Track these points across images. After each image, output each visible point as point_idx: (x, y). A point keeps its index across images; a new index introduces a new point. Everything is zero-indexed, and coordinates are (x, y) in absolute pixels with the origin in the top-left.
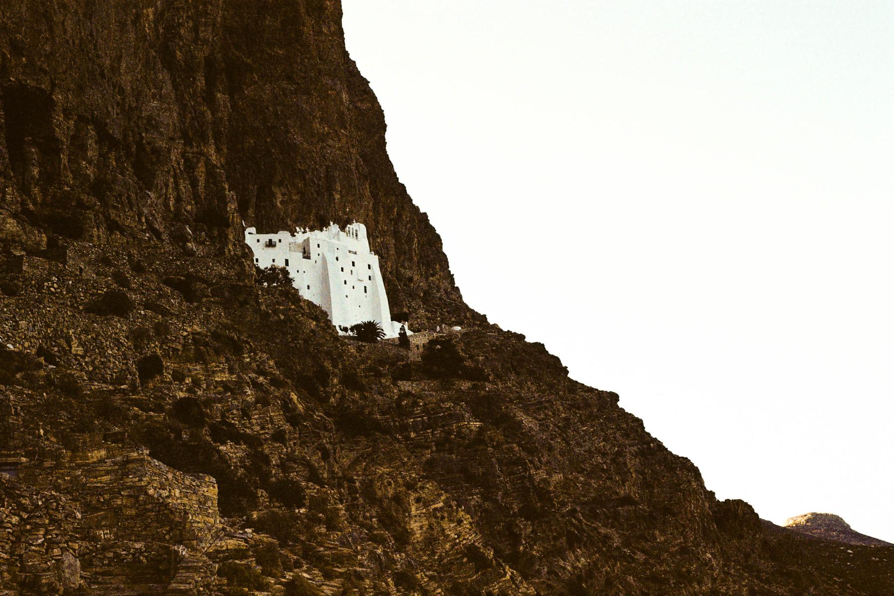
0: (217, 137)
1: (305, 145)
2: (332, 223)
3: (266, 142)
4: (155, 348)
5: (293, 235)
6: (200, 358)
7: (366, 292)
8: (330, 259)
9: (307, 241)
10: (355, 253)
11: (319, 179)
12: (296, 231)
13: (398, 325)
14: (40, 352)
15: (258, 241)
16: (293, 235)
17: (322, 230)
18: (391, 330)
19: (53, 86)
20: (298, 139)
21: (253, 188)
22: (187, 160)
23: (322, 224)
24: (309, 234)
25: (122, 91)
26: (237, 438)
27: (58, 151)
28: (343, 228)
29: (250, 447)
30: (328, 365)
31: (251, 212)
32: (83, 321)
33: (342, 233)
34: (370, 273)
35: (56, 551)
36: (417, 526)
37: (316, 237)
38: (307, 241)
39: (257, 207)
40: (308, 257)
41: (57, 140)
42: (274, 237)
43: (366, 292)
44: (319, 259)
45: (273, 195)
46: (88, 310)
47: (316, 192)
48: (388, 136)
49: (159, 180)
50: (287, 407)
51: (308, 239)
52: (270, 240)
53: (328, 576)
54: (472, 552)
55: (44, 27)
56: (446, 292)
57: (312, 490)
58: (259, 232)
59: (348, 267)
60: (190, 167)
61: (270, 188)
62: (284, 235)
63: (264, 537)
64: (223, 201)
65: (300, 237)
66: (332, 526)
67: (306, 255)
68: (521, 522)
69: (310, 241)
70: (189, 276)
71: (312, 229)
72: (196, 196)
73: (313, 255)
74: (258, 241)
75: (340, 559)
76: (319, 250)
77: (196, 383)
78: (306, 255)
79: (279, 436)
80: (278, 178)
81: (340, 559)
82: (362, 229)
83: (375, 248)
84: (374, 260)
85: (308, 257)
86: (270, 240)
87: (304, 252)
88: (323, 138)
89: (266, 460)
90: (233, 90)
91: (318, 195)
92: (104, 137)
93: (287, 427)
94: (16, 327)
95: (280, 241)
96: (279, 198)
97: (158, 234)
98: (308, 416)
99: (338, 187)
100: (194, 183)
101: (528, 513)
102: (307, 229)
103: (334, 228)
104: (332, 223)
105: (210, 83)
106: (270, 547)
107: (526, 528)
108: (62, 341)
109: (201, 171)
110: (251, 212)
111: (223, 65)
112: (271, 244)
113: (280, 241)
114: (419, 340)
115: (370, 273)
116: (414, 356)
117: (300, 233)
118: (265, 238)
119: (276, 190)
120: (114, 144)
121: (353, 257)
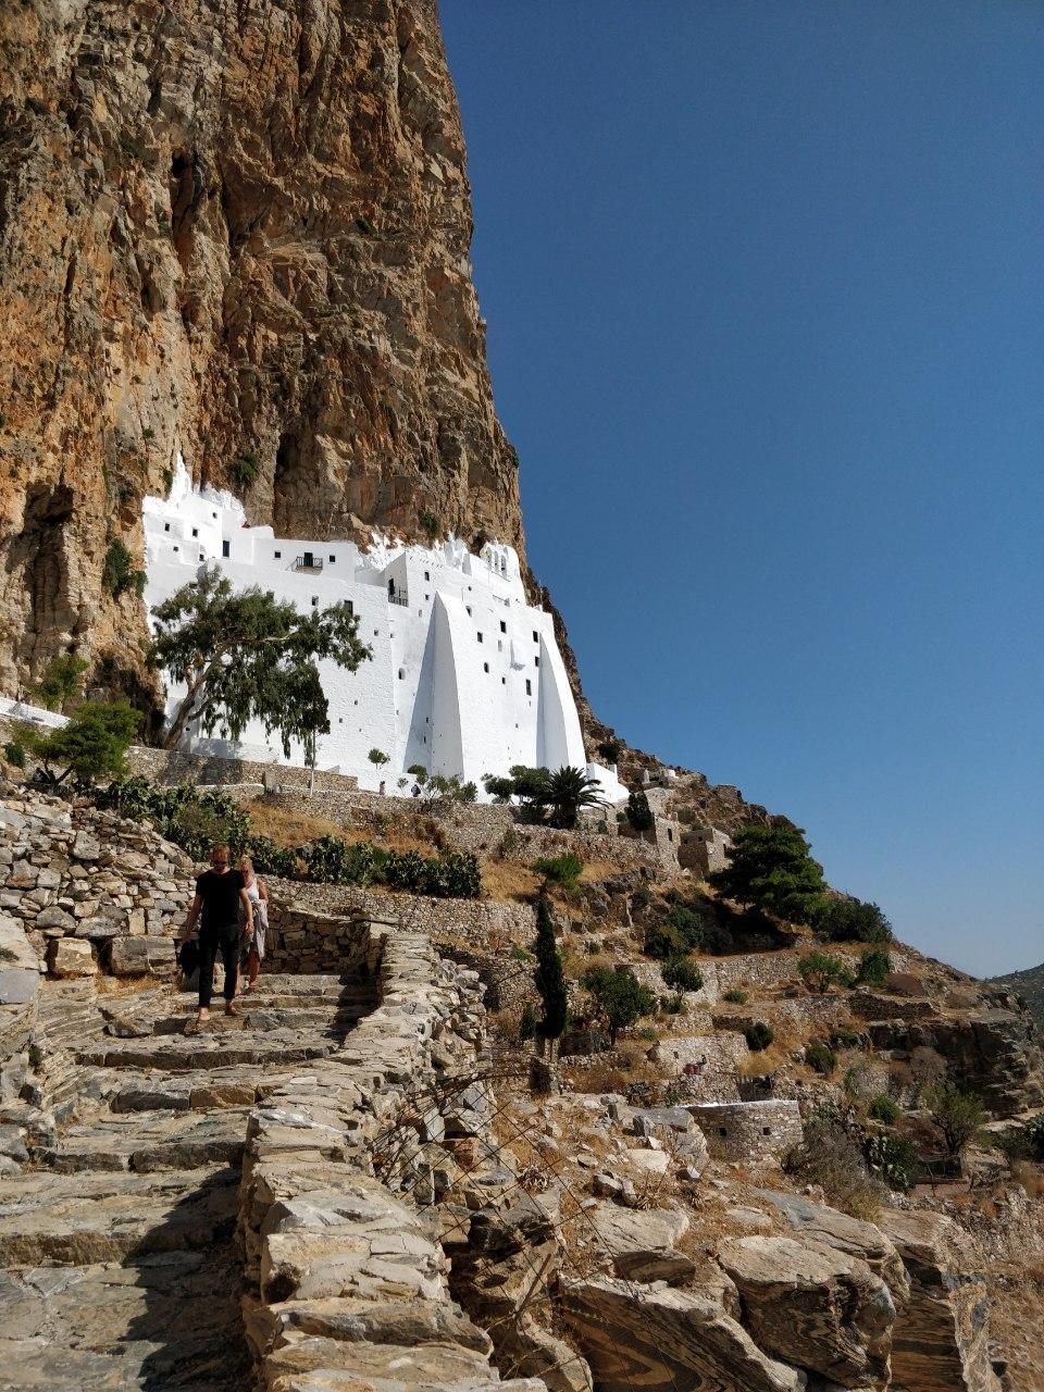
0: (188, 314)
1: (395, 361)
2: (451, 535)
3: (307, 340)
5: (364, 550)
8: (454, 608)
10: (507, 603)
12: (371, 541)
15: (278, 555)
16: (364, 550)
20: (383, 345)
21: (270, 434)
31: (263, 488)
33: (473, 557)
37: (419, 557)
39: (279, 482)
40: (403, 602)
42: (320, 550)
44: (428, 608)
45: (317, 452)
47: (419, 462)
52: (308, 558)
59: (493, 634)
61: (313, 438)
62: (345, 549)
67: (396, 593)
69: (408, 563)
73: (415, 596)
74: (278, 555)
78: (396, 593)
80: (329, 418)
84: (544, 622)
85: (403, 602)
86: (308, 558)
87: (392, 590)
88: (430, 361)
90: (239, 238)
91: (421, 469)
95: (332, 559)
96: (333, 460)
99: (464, 461)
102: (398, 541)
104: (451, 535)
111: (216, 178)
113: (332, 559)
115: (535, 649)
117: (382, 548)
118: (295, 548)
119: (325, 442)
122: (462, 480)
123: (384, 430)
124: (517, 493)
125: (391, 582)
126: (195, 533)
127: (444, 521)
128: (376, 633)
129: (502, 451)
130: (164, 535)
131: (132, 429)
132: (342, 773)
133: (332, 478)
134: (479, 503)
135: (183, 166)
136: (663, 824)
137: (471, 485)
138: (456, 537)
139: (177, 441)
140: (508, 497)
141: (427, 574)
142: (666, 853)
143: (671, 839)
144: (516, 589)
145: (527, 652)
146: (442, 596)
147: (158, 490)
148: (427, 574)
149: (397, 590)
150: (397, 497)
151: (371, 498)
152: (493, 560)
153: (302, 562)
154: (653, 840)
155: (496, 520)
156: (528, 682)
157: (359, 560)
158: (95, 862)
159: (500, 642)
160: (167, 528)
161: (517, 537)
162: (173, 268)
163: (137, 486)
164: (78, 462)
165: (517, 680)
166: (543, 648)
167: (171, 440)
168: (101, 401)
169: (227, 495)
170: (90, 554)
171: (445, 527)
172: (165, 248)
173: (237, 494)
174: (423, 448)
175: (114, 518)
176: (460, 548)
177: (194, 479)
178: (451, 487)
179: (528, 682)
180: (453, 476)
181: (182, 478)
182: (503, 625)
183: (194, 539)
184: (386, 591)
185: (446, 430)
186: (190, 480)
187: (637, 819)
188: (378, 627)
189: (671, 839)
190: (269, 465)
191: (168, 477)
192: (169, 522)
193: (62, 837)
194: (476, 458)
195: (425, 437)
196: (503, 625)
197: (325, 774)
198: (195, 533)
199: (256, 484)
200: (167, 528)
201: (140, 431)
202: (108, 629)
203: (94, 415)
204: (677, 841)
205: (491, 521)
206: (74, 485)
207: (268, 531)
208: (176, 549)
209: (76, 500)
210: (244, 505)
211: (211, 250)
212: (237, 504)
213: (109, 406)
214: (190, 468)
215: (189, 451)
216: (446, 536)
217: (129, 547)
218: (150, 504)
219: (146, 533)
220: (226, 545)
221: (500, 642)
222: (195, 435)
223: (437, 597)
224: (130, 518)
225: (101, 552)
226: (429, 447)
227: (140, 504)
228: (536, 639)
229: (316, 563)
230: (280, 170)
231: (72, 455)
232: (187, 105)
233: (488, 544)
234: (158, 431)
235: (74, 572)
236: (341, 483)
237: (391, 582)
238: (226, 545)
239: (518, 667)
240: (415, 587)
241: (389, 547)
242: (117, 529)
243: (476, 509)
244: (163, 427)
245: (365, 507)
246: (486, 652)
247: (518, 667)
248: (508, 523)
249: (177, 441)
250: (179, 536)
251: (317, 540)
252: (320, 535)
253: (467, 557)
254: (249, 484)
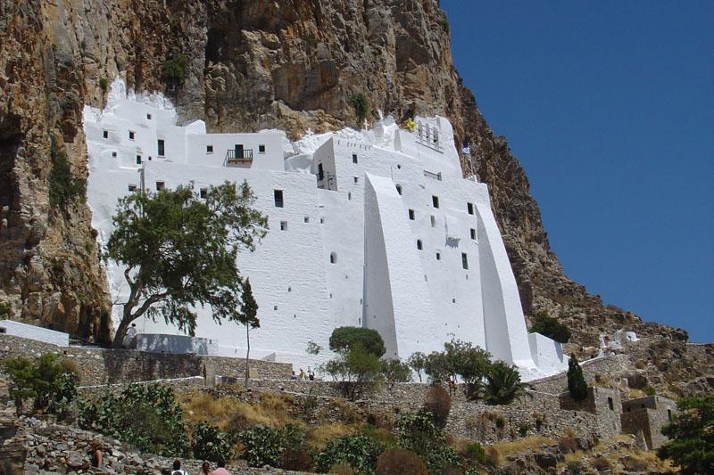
7: (465, 266)
8: (384, 186)
9: (328, 148)
10: (439, 176)
11: (349, 16)
15: (210, 149)
16: (294, 138)
17: (358, 127)
23: (361, 113)
24: (327, 135)
28: (402, 123)
33: (403, 133)
34: (472, 222)
37: (347, 139)
38: (328, 148)
42: (250, 141)
43: (465, 266)
45: (245, 45)
47: (345, 43)
51: (331, 140)
52: (239, 149)
56: (543, 263)
58: (215, 126)
62: (273, 137)
65: (311, 143)
67: (324, 177)
69: (335, 146)
71: (337, 124)
74: (210, 149)
76: (355, 170)
78: (324, 177)
84: (479, 193)
86: (239, 149)
87: (321, 176)
91: (347, 49)
95: (262, 149)
96: (260, 50)
112: (239, 156)
113: (262, 149)
117: (309, 131)
118: (226, 141)
119: (251, 36)
121: (434, 188)
122: (389, 58)
123: (308, 18)
124: (450, 60)
125: (320, 166)
126: (132, 136)
127: (374, 99)
128: (306, 220)
129: (431, 18)
130: (102, 143)
131: (67, 46)
132: (277, 360)
133: (259, 68)
134: (409, 75)
136: (601, 394)
137: (399, 61)
138: (385, 115)
139: (110, 48)
140: (439, 62)
141: (355, 157)
142: (607, 425)
143: (612, 408)
144: (448, 160)
146: (369, 176)
147: (95, 99)
148: (355, 157)
149: (325, 174)
150: (323, 81)
151: (298, 84)
152: (424, 133)
153: (233, 155)
154: (591, 408)
155: (427, 91)
156: (464, 256)
157: (288, 147)
158: (79, 467)
159: (432, 218)
160: (106, 135)
161: (450, 105)
163: (76, 98)
164: (24, 90)
165: (453, 255)
166: (480, 223)
167: (104, 48)
168: (39, 27)
169: (160, 97)
170: (37, 172)
171: (374, 106)
173: (167, 94)
174: (348, 28)
175: (57, 132)
176: (389, 127)
177: (129, 83)
178: (378, 67)
179: (464, 256)
180: (380, 53)
181: (118, 85)
182: (435, 200)
183: (131, 141)
184: (314, 177)
185: (372, 6)
186: (124, 84)
187: (577, 392)
188: (309, 214)
189: (612, 408)
191: (104, 86)
192: (106, 129)
193: (62, 454)
194: (403, 31)
195: (349, 16)
196: (435, 200)
197: (261, 362)
198: (132, 136)
199: (187, 81)
200: (106, 135)
201: (75, 44)
202: (57, 237)
203: (34, 43)
204: (618, 408)
205: (421, 93)
206: (21, 111)
207: (199, 126)
208: (115, 155)
209: (23, 125)
210: (176, 105)
212: (170, 105)
213: (46, 25)
214: (124, 73)
215: (123, 56)
216: (375, 114)
217: (72, 158)
218: (89, 114)
219: (88, 142)
220: (161, 143)
221: (432, 218)
222: (127, 40)
223: (367, 180)
224: (71, 131)
225: (47, 170)
226: (354, 27)
227: (80, 116)
228: (471, 211)
229: (246, 155)
231: (17, 84)
233: (417, 118)
234: (91, 43)
235: (24, 190)
236: (268, 74)
237: (320, 166)
238: (161, 143)
239: (452, 242)
240: (343, 168)
241: (317, 132)
242: (61, 142)
243: (406, 81)
244: (97, 38)
245: (292, 94)
247: (452, 242)
248: (440, 92)
249: (110, 48)
250: (116, 141)
251: (247, 131)
252: (249, 125)
253: (397, 132)
254: (180, 85)
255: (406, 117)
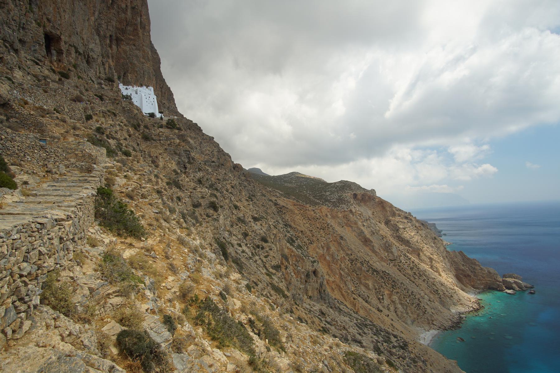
0: (112, 57)
4: (90, 112)
6: (104, 117)
8: (143, 95)
13: (160, 114)
14: (55, 110)
18: (158, 115)
19: (61, 34)
20: (136, 62)
22: (103, 62)
23: (141, 86)
25: (83, 39)
26: (114, 138)
27: (62, 53)
29: (117, 141)
30: (140, 123)
32: (68, 103)
35: (58, 164)
36: (161, 164)
41: (62, 50)
46: (70, 100)
48: (161, 66)
49: (95, 66)
50: (128, 131)
53: (136, 174)
54: (175, 171)
55: (58, 16)
57: (133, 153)
59: (148, 98)
60: (103, 64)
62: (130, 87)
63: (119, 164)
64: (113, 75)
65: (135, 88)
66: (138, 162)
68: (187, 164)
70: (102, 94)
71: (139, 86)
72: (105, 73)
75: (139, 171)
77: (102, 123)
79: (125, 139)
80: (129, 72)
81: (139, 171)
82: (152, 89)
83: (155, 94)
84: (155, 97)
88: (143, 63)
89: (122, 145)
90: (118, 45)
92: (77, 51)
93: (128, 137)
94: (47, 102)
96: (130, 77)
97: (93, 82)
98: (134, 134)
100: (105, 69)
101: (189, 162)
103: (145, 87)
105: (111, 41)
106: (120, 167)
107: (188, 165)
108: (62, 108)
109: (107, 66)
110: (121, 79)
112: (127, 89)
114: (166, 119)
116: (164, 123)
118: (125, 87)
119: (129, 75)
120: (80, 54)
135: (111, 36)
145: (152, 100)
162: (110, 51)
172: (109, 49)
187: (161, 118)
190: (122, 77)
211: (114, 47)
230: (123, 36)
232: (111, 29)
240: (138, 92)
246: (147, 100)
255: (147, 87)
